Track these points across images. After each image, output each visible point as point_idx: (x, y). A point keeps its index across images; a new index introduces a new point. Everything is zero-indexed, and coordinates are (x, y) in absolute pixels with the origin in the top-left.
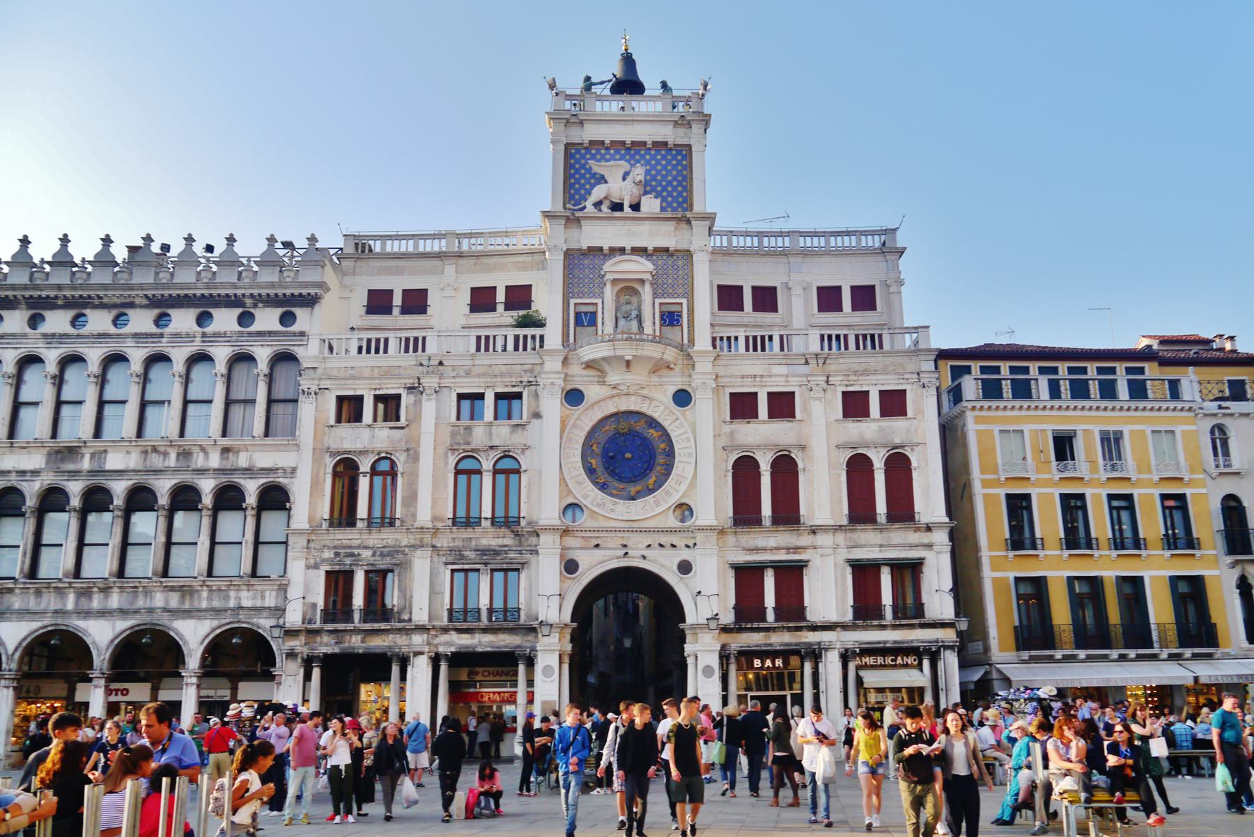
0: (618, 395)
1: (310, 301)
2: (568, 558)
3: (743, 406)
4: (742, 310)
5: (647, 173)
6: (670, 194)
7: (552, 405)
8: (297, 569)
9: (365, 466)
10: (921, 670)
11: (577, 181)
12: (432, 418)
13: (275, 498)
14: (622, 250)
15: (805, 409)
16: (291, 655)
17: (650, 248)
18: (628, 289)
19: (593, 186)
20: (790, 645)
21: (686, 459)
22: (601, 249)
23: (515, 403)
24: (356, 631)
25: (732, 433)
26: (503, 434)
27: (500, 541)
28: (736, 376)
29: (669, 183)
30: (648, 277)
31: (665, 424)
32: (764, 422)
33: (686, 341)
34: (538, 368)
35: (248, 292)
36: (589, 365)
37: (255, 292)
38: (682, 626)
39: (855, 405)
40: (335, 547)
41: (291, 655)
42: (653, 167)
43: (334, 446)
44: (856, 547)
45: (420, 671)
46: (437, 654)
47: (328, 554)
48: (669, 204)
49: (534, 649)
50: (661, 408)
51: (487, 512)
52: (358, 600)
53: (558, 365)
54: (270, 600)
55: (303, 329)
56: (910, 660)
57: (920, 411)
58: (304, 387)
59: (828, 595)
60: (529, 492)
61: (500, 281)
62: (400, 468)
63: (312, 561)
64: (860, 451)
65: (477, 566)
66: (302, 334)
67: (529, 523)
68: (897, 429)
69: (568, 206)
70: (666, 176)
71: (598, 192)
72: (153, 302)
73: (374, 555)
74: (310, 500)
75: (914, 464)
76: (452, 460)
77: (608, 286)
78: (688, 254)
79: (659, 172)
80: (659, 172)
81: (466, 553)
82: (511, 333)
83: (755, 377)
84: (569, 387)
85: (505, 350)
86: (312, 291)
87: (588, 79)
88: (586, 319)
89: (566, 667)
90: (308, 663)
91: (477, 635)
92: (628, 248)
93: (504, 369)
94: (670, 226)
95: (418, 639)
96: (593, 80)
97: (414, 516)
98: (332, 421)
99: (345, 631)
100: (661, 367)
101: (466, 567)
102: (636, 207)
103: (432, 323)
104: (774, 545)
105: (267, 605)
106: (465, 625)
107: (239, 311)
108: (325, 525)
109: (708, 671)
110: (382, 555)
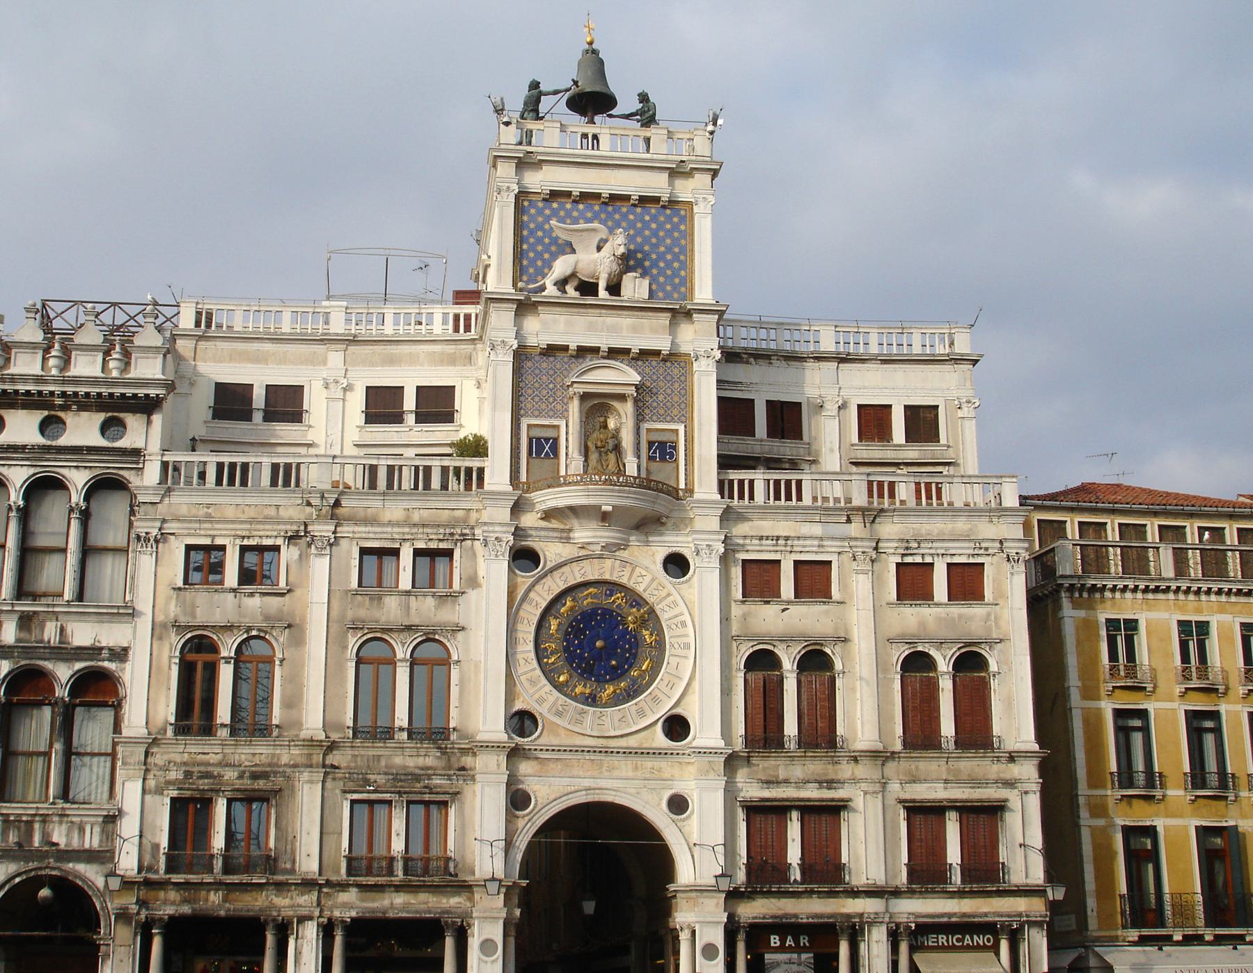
0: (587, 557)
1: (147, 406)
2: (514, 788)
3: (759, 580)
4: (752, 433)
5: (630, 239)
6: (662, 272)
8: (130, 794)
9: (228, 647)
10: (996, 949)
11: (532, 248)
14: (595, 350)
15: (844, 586)
16: (123, 916)
17: (635, 350)
19: (554, 257)
20: (821, 916)
21: (680, 652)
22: (565, 348)
23: (441, 564)
24: (218, 885)
25: (745, 617)
26: (425, 609)
27: (421, 761)
29: (661, 257)
33: (682, 486)
34: (474, 515)
35: (57, 389)
36: (548, 515)
37: (70, 389)
38: (672, 887)
39: (913, 582)
40: (185, 764)
41: (123, 916)
42: (639, 233)
43: (183, 620)
44: (914, 780)
46: (330, 919)
47: (173, 775)
49: (467, 915)
50: (648, 579)
52: (218, 842)
53: (504, 514)
54: (92, 840)
55: (139, 444)
56: (979, 940)
57: (1000, 594)
59: (870, 846)
60: (461, 693)
61: (410, 379)
62: (279, 655)
63: (151, 783)
64: (920, 648)
65: (387, 796)
66: (136, 454)
67: (464, 736)
68: (971, 618)
69: (520, 285)
70: (657, 246)
71: (561, 266)
73: (241, 777)
74: (148, 695)
75: (993, 667)
76: (353, 642)
77: (576, 402)
81: (372, 777)
82: (436, 464)
83: (778, 538)
85: (427, 486)
86: (153, 392)
87: (535, 85)
88: (544, 447)
89: (512, 940)
90: (145, 932)
91: (386, 895)
92: (604, 348)
93: (425, 513)
94: (665, 319)
97: (298, 724)
98: (180, 583)
99: (202, 884)
100: (647, 524)
101: (373, 796)
102: (614, 289)
103: (311, 437)
104: (801, 777)
105: (87, 846)
106: (371, 880)
107: (39, 415)
108: (170, 733)
110: (255, 776)
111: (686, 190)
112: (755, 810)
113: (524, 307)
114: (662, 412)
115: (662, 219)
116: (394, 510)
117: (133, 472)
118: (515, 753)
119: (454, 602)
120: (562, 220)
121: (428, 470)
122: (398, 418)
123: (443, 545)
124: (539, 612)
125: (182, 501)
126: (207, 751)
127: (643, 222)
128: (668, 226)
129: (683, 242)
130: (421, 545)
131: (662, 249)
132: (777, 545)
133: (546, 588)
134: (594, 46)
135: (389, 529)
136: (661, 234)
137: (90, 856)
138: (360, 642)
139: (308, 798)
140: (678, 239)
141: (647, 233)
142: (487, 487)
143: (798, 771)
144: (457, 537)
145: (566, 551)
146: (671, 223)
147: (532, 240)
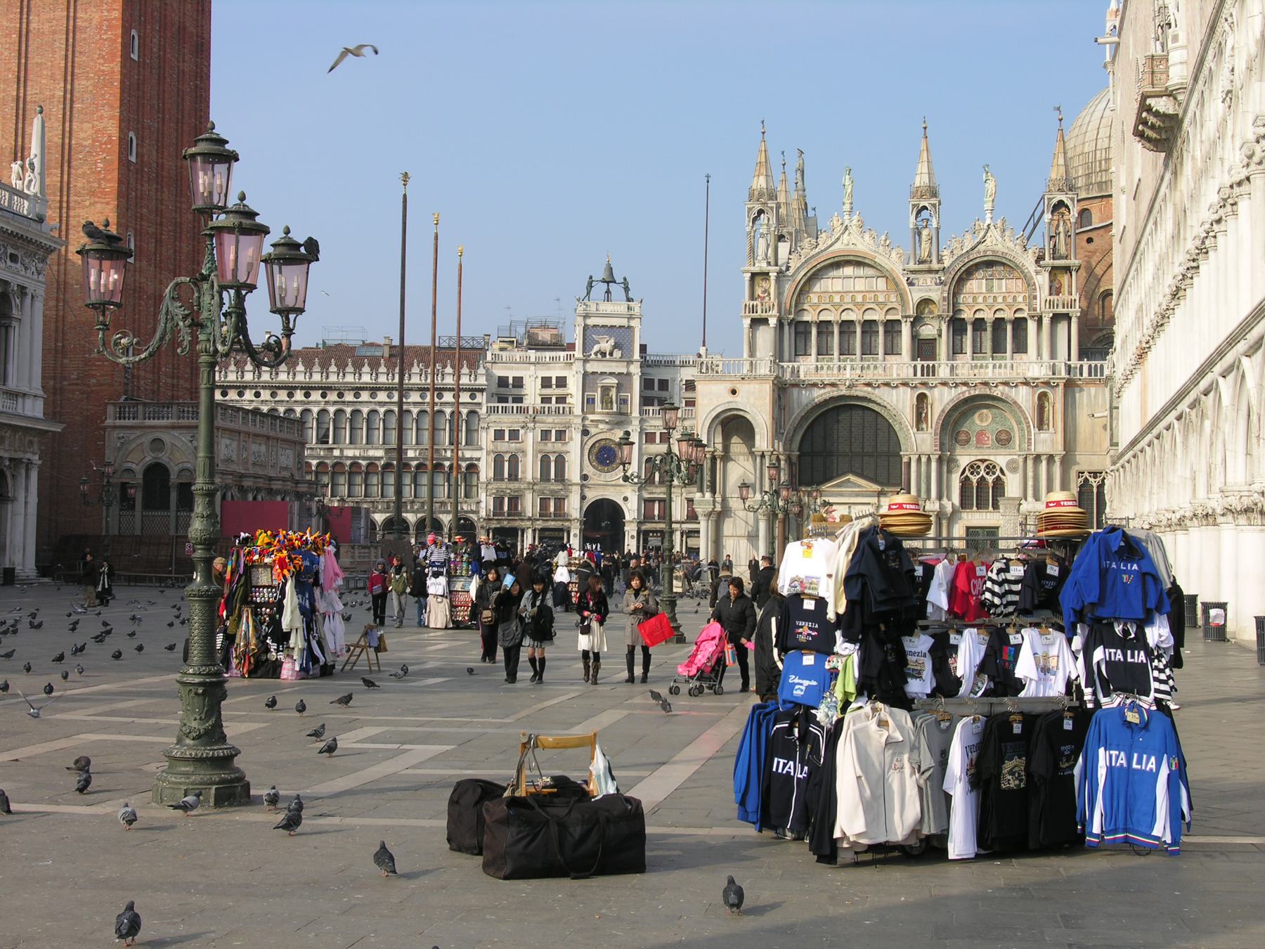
1: (482, 391)
7: (577, 436)
12: (530, 439)
13: (473, 468)
18: (606, 389)
45: (529, 534)
51: (553, 476)
71: (596, 348)
72: (419, 389)
74: (486, 470)
76: (540, 456)
88: (591, 401)
95: (529, 523)
102: (611, 354)
103: (526, 392)
109: (633, 537)
111: (633, 323)
112: (647, 501)
113: (586, 361)
116: (550, 419)
118: (582, 486)
125: (493, 417)
126: (503, 485)
137: (472, 512)
139: (529, 497)
143: (658, 490)
145: (597, 431)
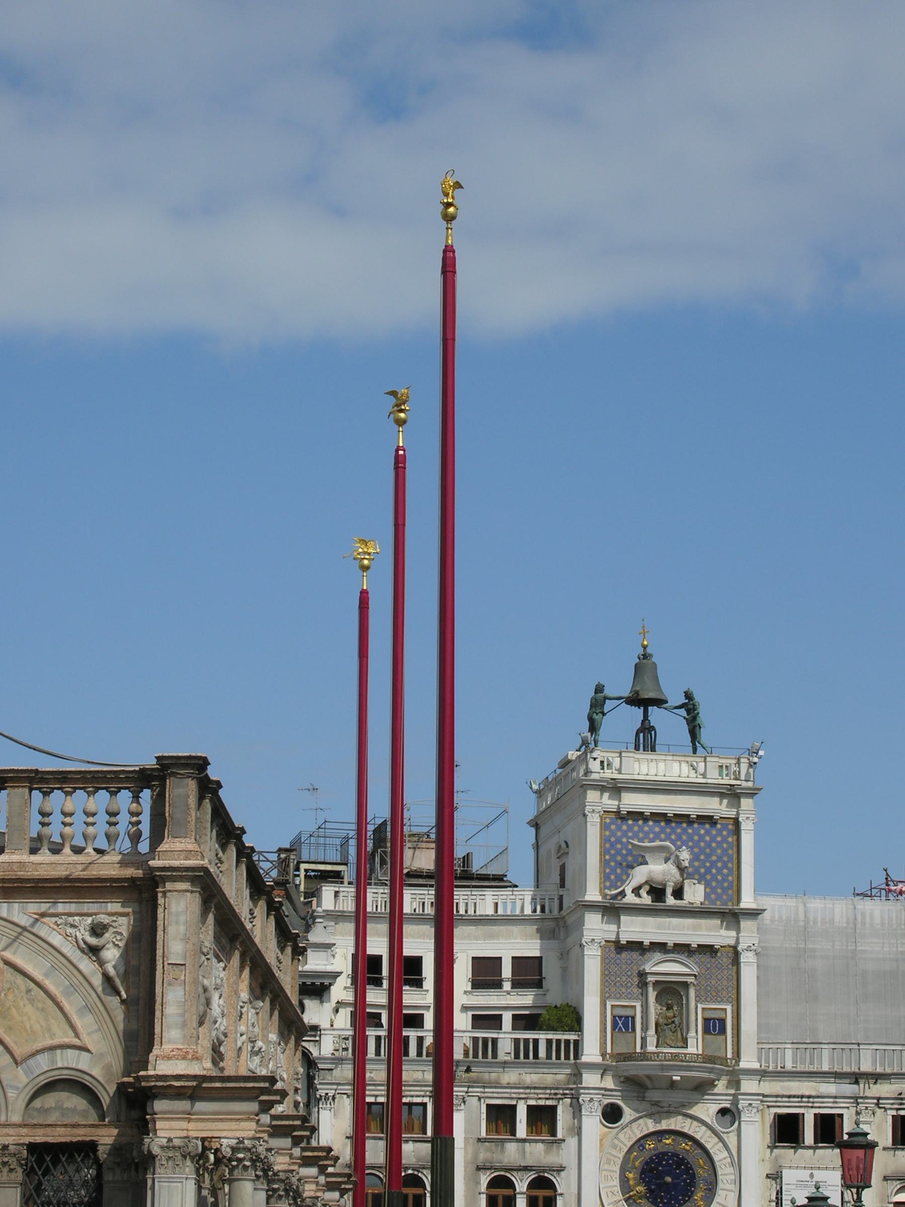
5: (690, 849)
28: (783, 1096)
29: (713, 864)
30: (690, 980)
31: (708, 1146)
32: (810, 1147)
33: (729, 1055)
42: (696, 844)
48: (713, 890)
58: (321, 1092)
70: (710, 855)
71: (640, 874)
76: (485, 1179)
77: (650, 989)
78: (735, 954)
79: (702, 851)
80: (702, 851)
82: (542, 1037)
83: (802, 1097)
84: (606, 1101)
85: (536, 1056)
86: (326, 982)
92: (670, 944)
96: (608, 692)
102: (678, 893)
114: (714, 994)
115: (714, 832)
117: (311, 1043)
119: (558, 1148)
120: (635, 836)
121: (536, 1042)
122: (497, 984)
123: (549, 1103)
124: (621, 1155)
127: (700, 835)
128: (719, 839)
129: (730, 852)
130: (532, 1102)
131: (714, 858)
132: (802, 1102)
133: (627, 1136)
134: (649, 650)
135: (508, 1090)
136: (714, 845)
138: (489, 1178)
140: (726, 850)
141: (702, 844)
142: (584, 1059)
144: (559, 1096)
146: (722, 835)
147: (613, 852)
